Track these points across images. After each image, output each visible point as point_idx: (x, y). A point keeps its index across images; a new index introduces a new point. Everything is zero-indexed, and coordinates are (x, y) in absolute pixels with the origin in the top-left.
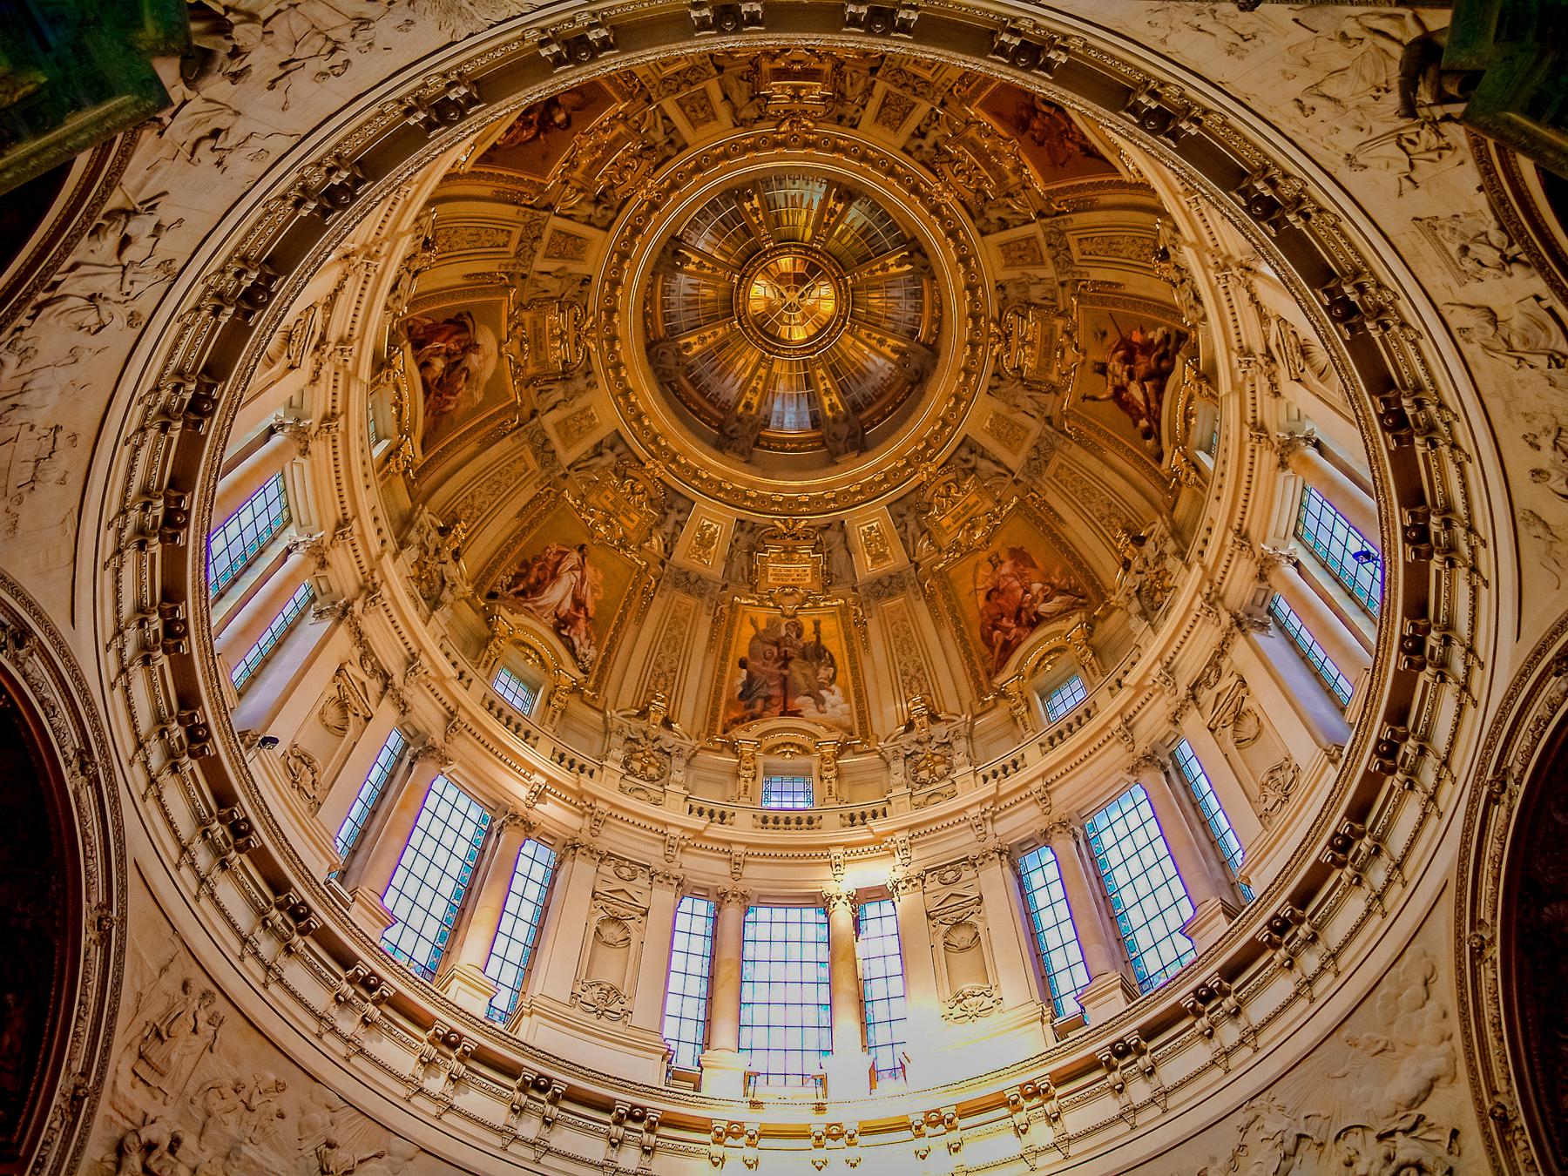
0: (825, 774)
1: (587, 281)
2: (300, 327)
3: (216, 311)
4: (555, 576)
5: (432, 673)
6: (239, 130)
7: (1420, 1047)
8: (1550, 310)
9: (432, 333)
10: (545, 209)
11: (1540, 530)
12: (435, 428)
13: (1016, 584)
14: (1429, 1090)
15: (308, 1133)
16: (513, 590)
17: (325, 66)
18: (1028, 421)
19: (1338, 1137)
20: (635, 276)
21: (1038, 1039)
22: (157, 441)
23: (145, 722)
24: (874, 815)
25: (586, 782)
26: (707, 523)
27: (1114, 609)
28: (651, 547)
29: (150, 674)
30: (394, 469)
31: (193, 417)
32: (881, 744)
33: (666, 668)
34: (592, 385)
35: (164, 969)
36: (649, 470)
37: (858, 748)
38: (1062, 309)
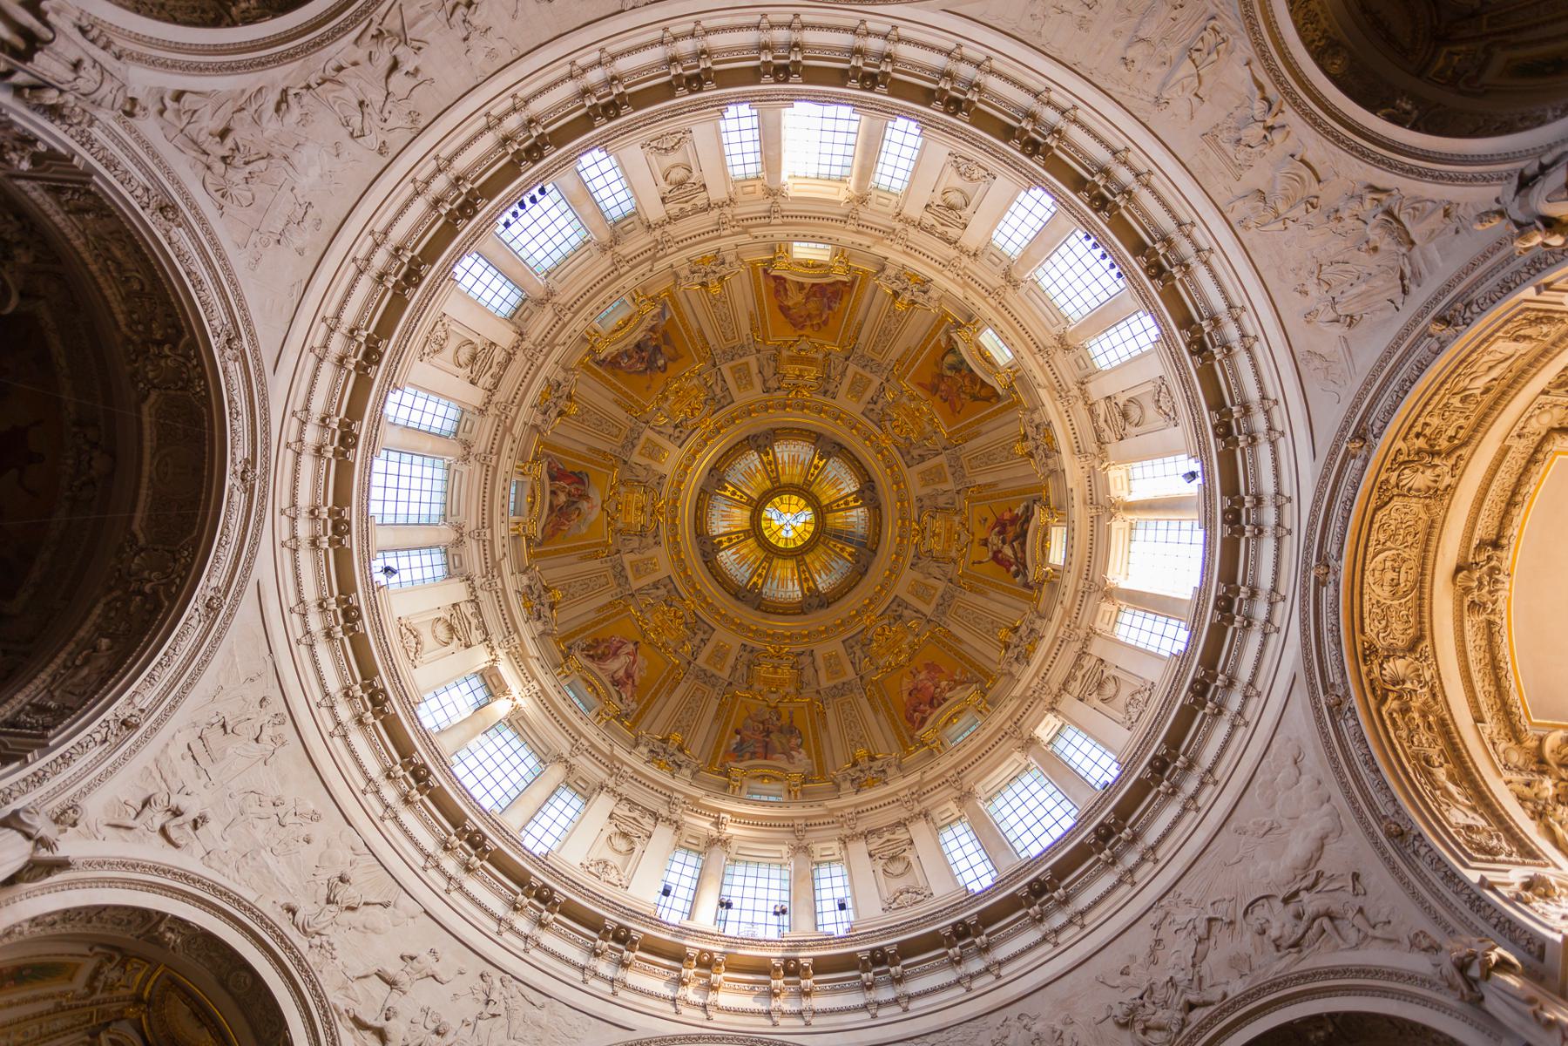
7: (1304, 816)
11: (1317, 362)
12: (553, 535)
14: (1322, 846)
15: (327, 864)
19: (1246, 913)
34: (658, 543)
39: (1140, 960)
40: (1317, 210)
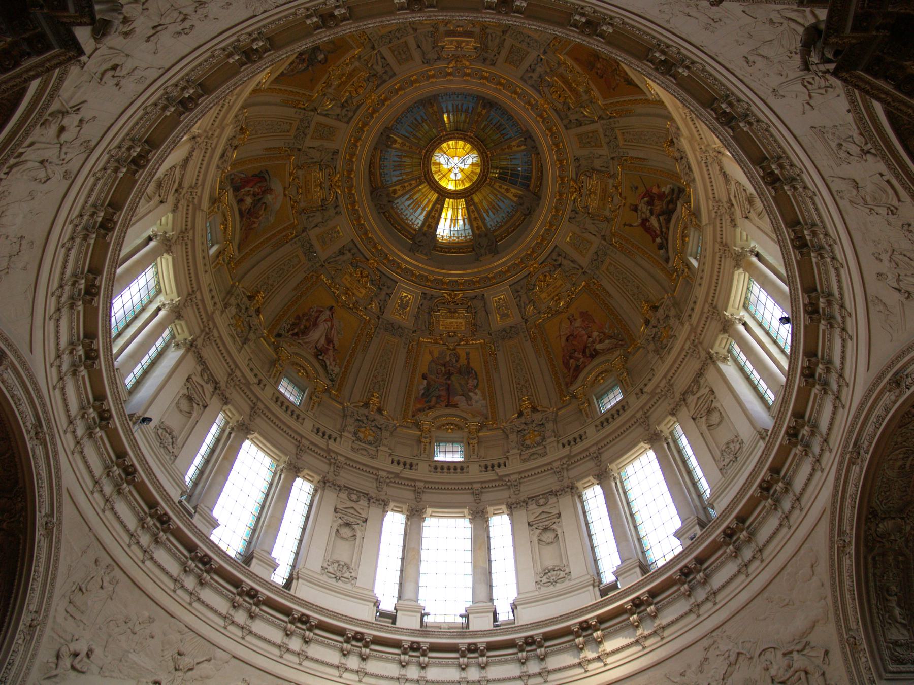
0: (471, 441)
1: (336, 152)
2: (166, 178)
3: (116, 170)
4: (315, 325)
5: (243, 381)
6: (129, 65)
8: (888, 181)
9: (246, 182)
10: (312, 110)
11: (881, 308)
12: (246, 238)
13: (584, 332)
14: (813, 627)
16: (291, 332)
17: (179, 29)
18: (592, 238)
20: (364, 152)
21: (590, 597)
22: (81, 245)
23: (74, 408)
24: (499, 466)
25: (332, 445)
26: (405, 294)
27: (640, 348)
28: (372, 308)
29: (77, 381)
30: (221, 262)
31: (102, 232)
32: (504, 424)
33: (380, 379)
35: (84, 552)
36: (371, 264)
37: (490, 427)
38: (612, 173)
39: (693, 669)
40: (895, 216)
